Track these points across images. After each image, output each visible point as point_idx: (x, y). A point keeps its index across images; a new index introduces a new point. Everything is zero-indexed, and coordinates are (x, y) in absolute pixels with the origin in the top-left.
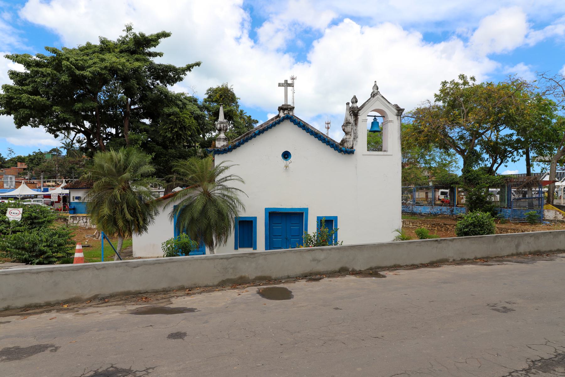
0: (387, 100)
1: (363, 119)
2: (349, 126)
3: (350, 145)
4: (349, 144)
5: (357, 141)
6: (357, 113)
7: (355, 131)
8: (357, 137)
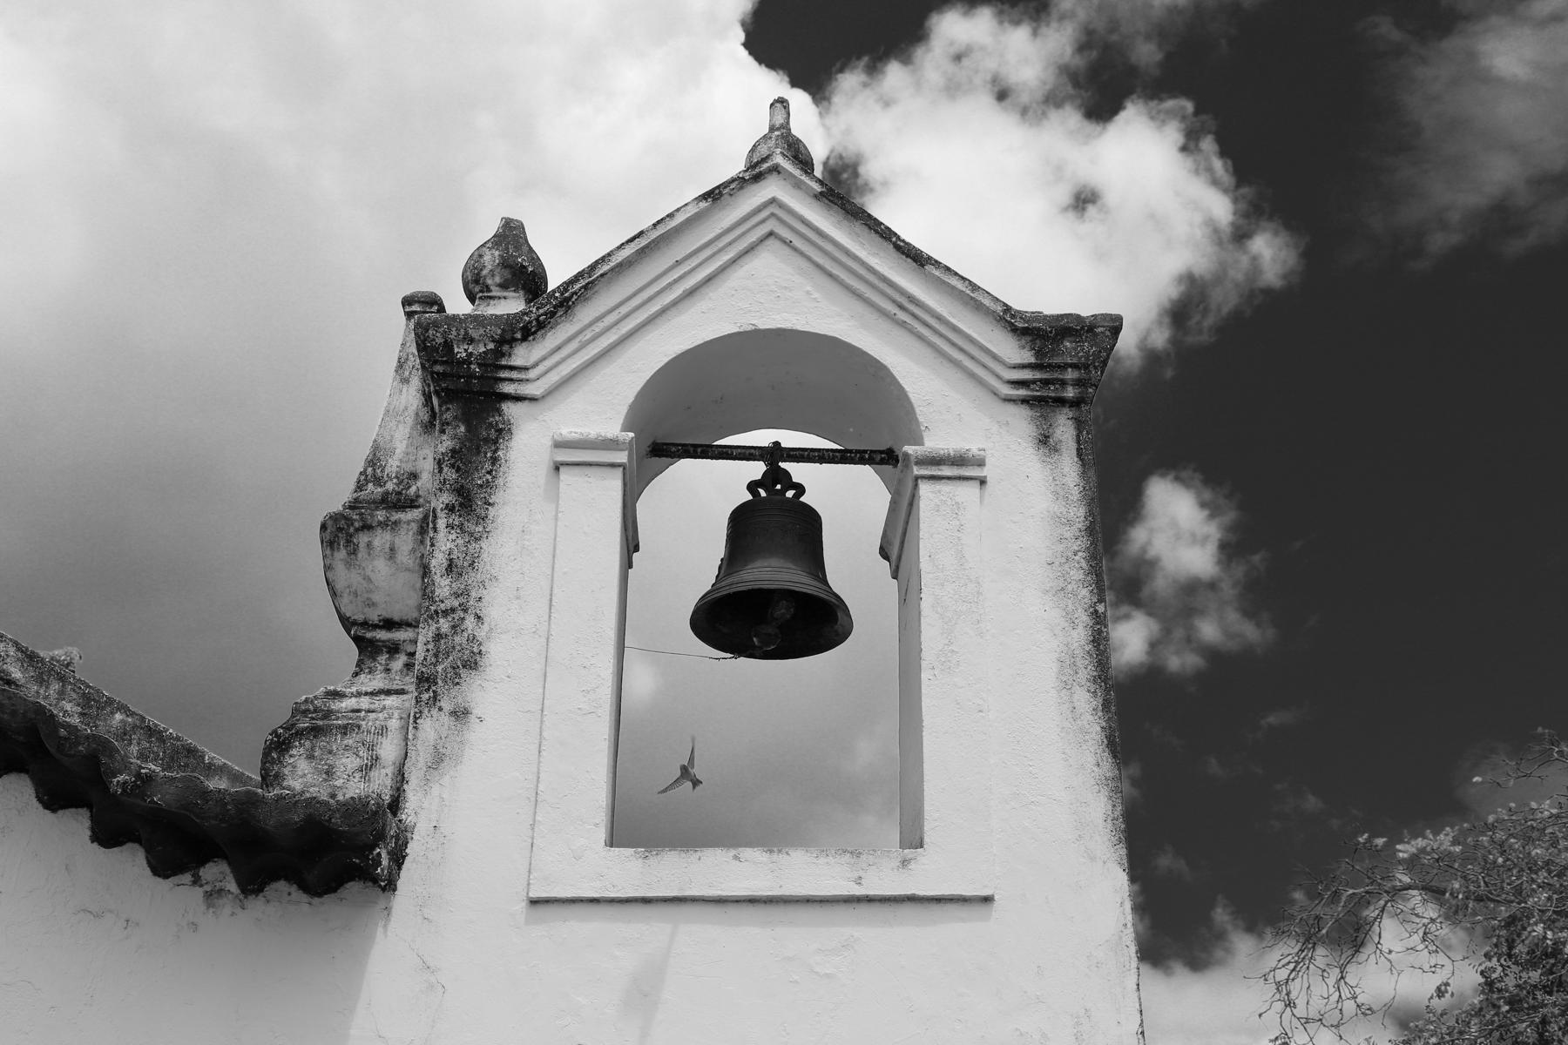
0: (886, 234)
1: (569, 431)
2: (381, 539)
3: (366, 770)
4: (348, 763)
5: (461, 714)
6: (494, 363)
7: (443, 587)
8: (472, 663)
